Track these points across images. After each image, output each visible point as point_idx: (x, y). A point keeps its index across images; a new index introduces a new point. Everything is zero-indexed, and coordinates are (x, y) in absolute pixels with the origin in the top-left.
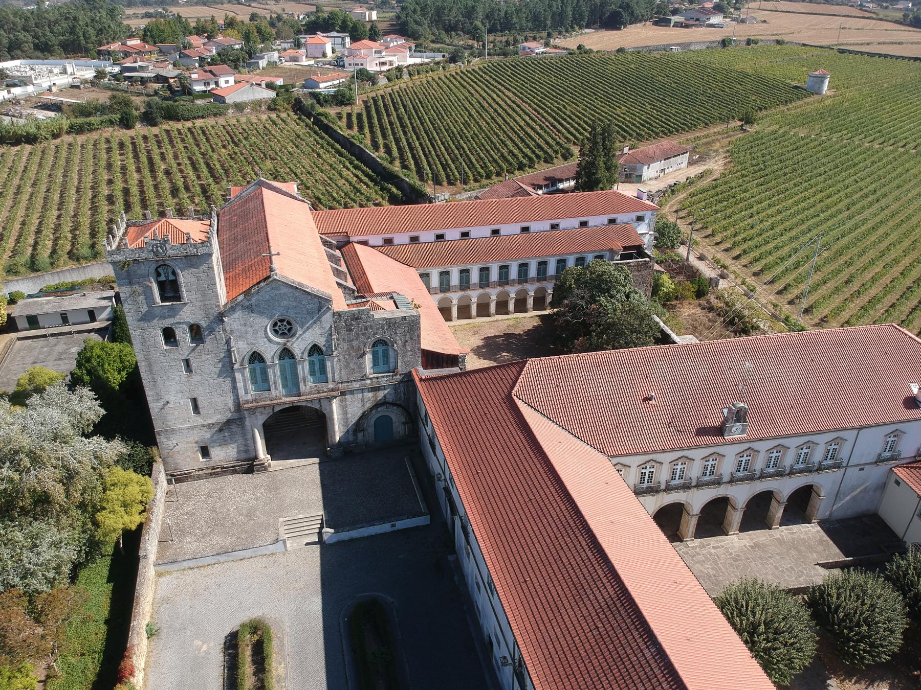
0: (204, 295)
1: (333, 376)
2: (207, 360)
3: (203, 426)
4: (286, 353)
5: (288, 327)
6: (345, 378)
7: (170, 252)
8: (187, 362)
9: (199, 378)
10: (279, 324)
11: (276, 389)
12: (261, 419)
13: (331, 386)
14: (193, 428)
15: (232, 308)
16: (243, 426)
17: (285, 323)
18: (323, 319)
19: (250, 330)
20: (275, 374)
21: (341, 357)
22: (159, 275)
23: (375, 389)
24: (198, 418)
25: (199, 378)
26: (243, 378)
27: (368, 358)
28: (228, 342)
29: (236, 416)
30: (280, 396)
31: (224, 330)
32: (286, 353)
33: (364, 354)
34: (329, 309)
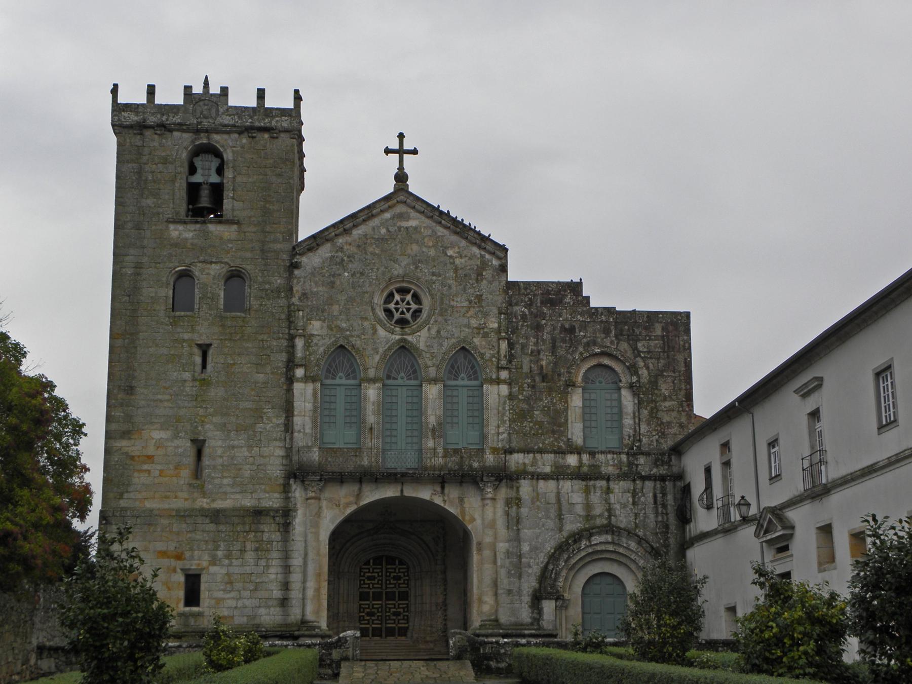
8: (204, 350)
10: (397, 297)
12: (330, 519)
17: (409, 297)
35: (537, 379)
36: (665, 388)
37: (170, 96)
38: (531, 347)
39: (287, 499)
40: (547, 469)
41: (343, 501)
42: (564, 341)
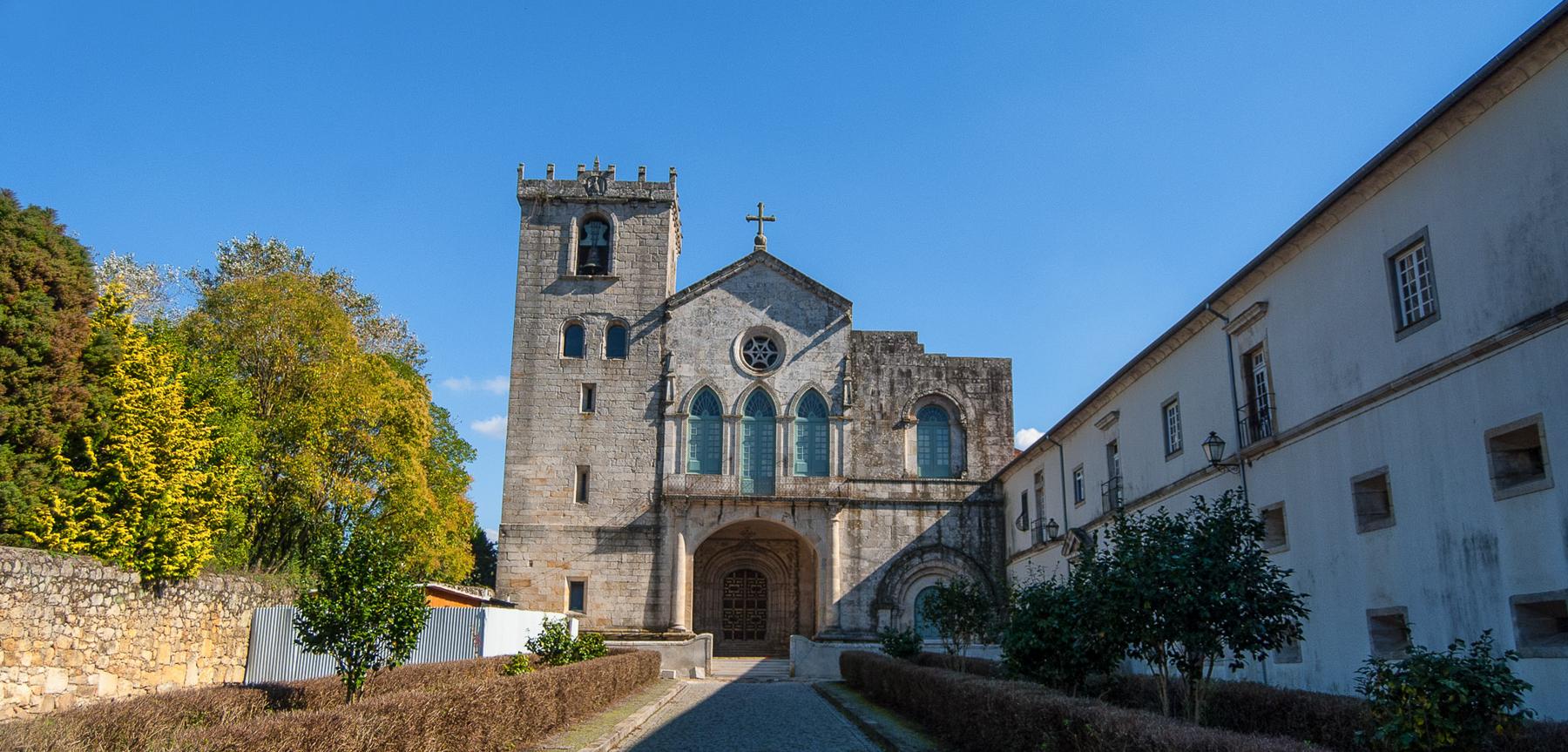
0: (643, 271)
1: (841, 464)
2: (624, 396)
3: (586, 529)
4: (760, 403)
5: (770, 353)
6: (861, 473)
7: (611, 192)
8: (590, 391)
9: (603, 425)
10: (756, 344)
11: (732, 472)
13: (834, 485)
14: (568, 531)
15: (684, 296)
16: (657, 545)
17: (765, 345)
18: (832, 339)
19: (707, 344)
20: (736, 438)
21: (859, 425)
22: (583, 235)
23: (919, 505)
24: (582, 513)
25: (603, 425)
26: (679, 436)
27: (910, 436)
28: (666, 358)
29: (650, 520)
30: (735, 479)
31: (663, 337)
32: (760, 403)
33: (903, 424)
34: (846, 321)
35: (878, 416)
36: (989, 424)
37: (566, 172)
38: (872, 388)
39: (658, 518)
40: (885, 496)
41: (707, 521)
42: (900, 383)
